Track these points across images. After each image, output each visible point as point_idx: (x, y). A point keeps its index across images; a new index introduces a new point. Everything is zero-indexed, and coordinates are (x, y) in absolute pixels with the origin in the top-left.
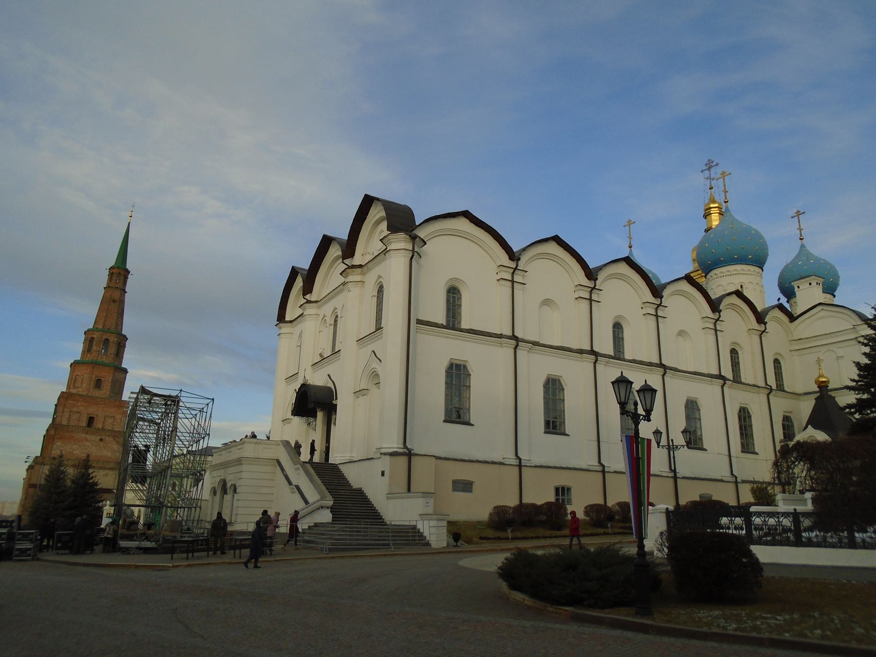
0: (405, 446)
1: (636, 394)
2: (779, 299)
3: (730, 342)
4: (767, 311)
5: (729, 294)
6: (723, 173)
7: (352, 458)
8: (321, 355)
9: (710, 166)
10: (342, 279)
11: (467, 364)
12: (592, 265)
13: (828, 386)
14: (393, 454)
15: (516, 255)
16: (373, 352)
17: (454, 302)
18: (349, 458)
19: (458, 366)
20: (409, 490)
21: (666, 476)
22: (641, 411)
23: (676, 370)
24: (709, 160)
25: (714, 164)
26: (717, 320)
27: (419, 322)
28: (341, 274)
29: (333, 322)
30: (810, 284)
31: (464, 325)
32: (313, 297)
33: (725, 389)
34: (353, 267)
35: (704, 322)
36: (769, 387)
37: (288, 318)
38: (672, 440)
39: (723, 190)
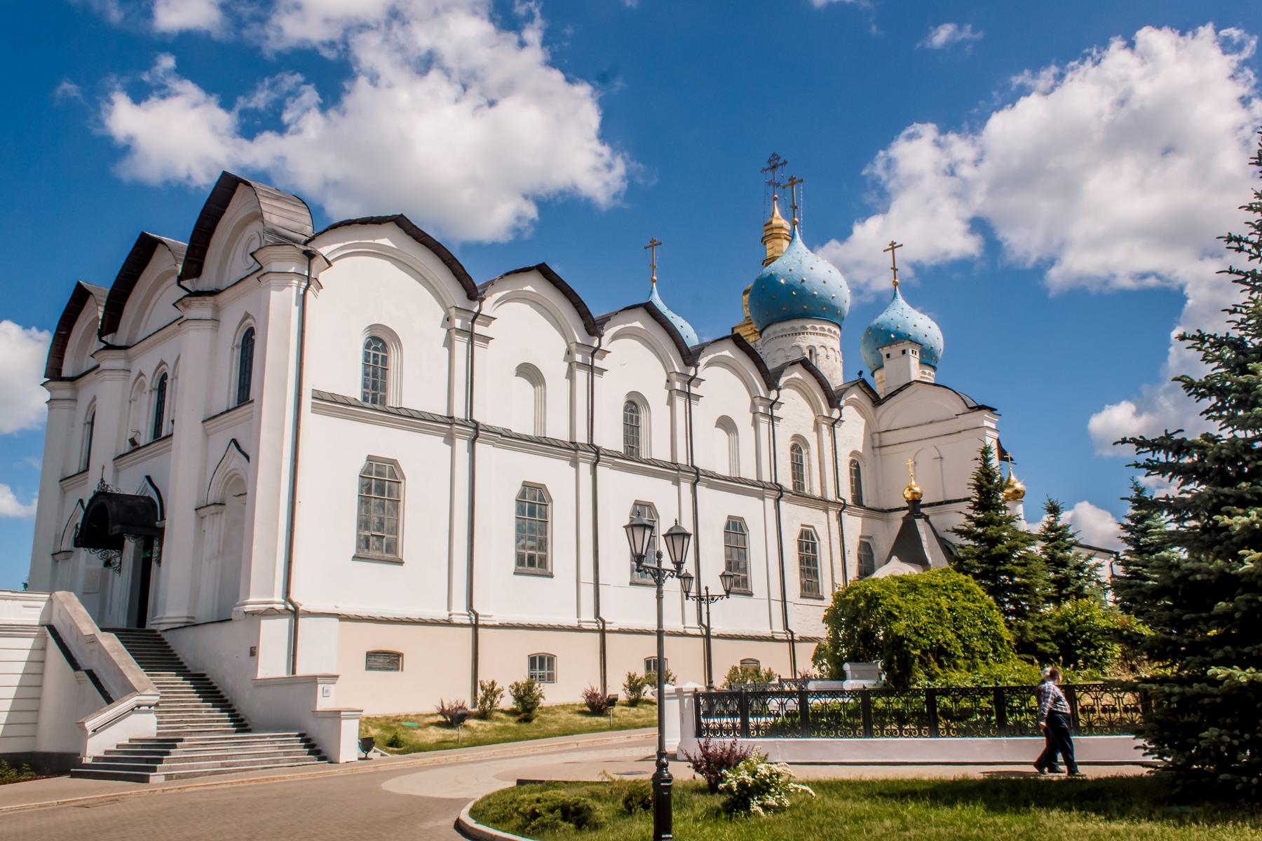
1: (662, 539)
2: (860, 373)
3: (791, 435)
4: (842, 392)
5: (793, 363)
6: (792, 179)
7: (192, 620)
8: (133, 442)
9: (775, 164)
10: (175, 313)
12: (596, 314)
13: (920, 501)
14: (271, 613)
15: (479, 291)
16: (234, 441)
17: (376, 362)
18: (185, 620)
21: (694, 633)
22: (667, 563)
23: (713, 475)
24: (774, 155)
25: (781, 161)
27: (318, 396)
28: (174, 305)
29: (156, 385)
30: (904, 352)
31: (392, 402)
32: (121, 337)
33: (782, 503)
35: (753, 405)
36: (842, 502)
37: (67, 371)
38: (707, 588)
39: (791, 204)
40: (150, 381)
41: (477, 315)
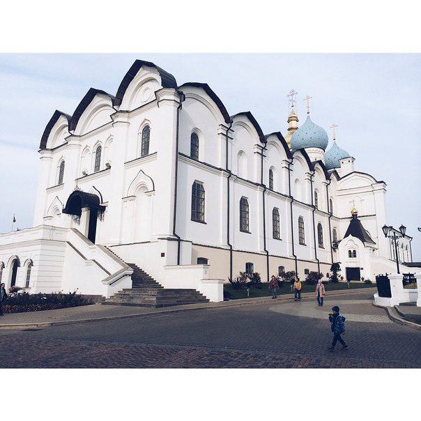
0: (175, 234)
8: (84, 173)
11: (203, 185)
14: (169, 239)
19: (199, 185)
20: (178, 264)
26: (312, 175)
27: (180, 154)
32: (77, 132)
34: (121, 111)
37: (49, 146)
40: (93, 149)
41: (229, 129)
